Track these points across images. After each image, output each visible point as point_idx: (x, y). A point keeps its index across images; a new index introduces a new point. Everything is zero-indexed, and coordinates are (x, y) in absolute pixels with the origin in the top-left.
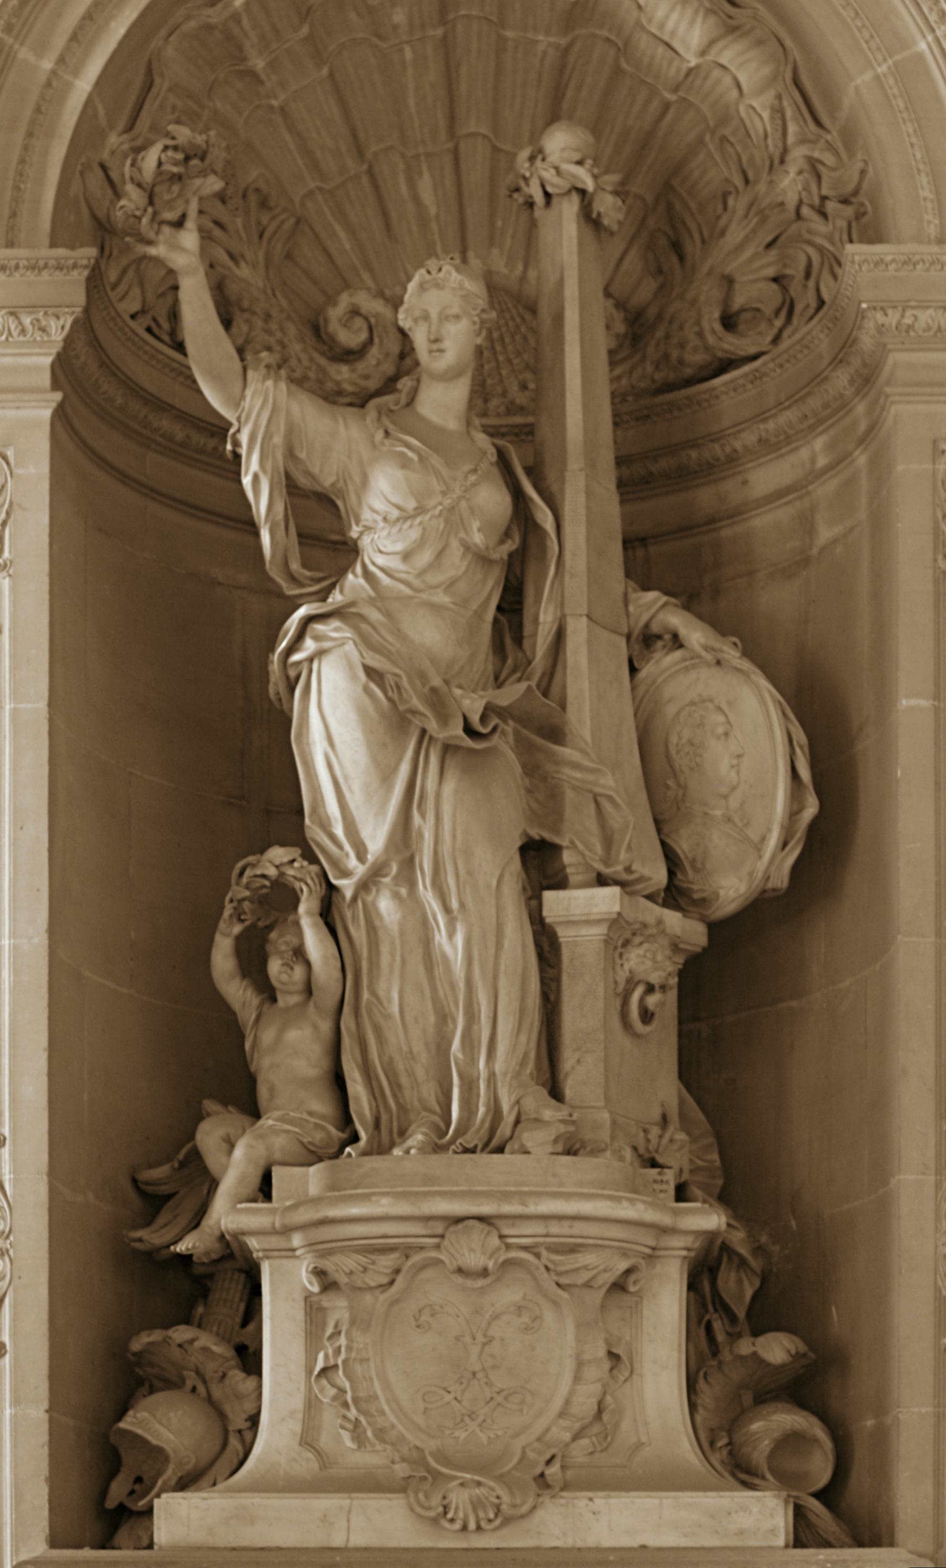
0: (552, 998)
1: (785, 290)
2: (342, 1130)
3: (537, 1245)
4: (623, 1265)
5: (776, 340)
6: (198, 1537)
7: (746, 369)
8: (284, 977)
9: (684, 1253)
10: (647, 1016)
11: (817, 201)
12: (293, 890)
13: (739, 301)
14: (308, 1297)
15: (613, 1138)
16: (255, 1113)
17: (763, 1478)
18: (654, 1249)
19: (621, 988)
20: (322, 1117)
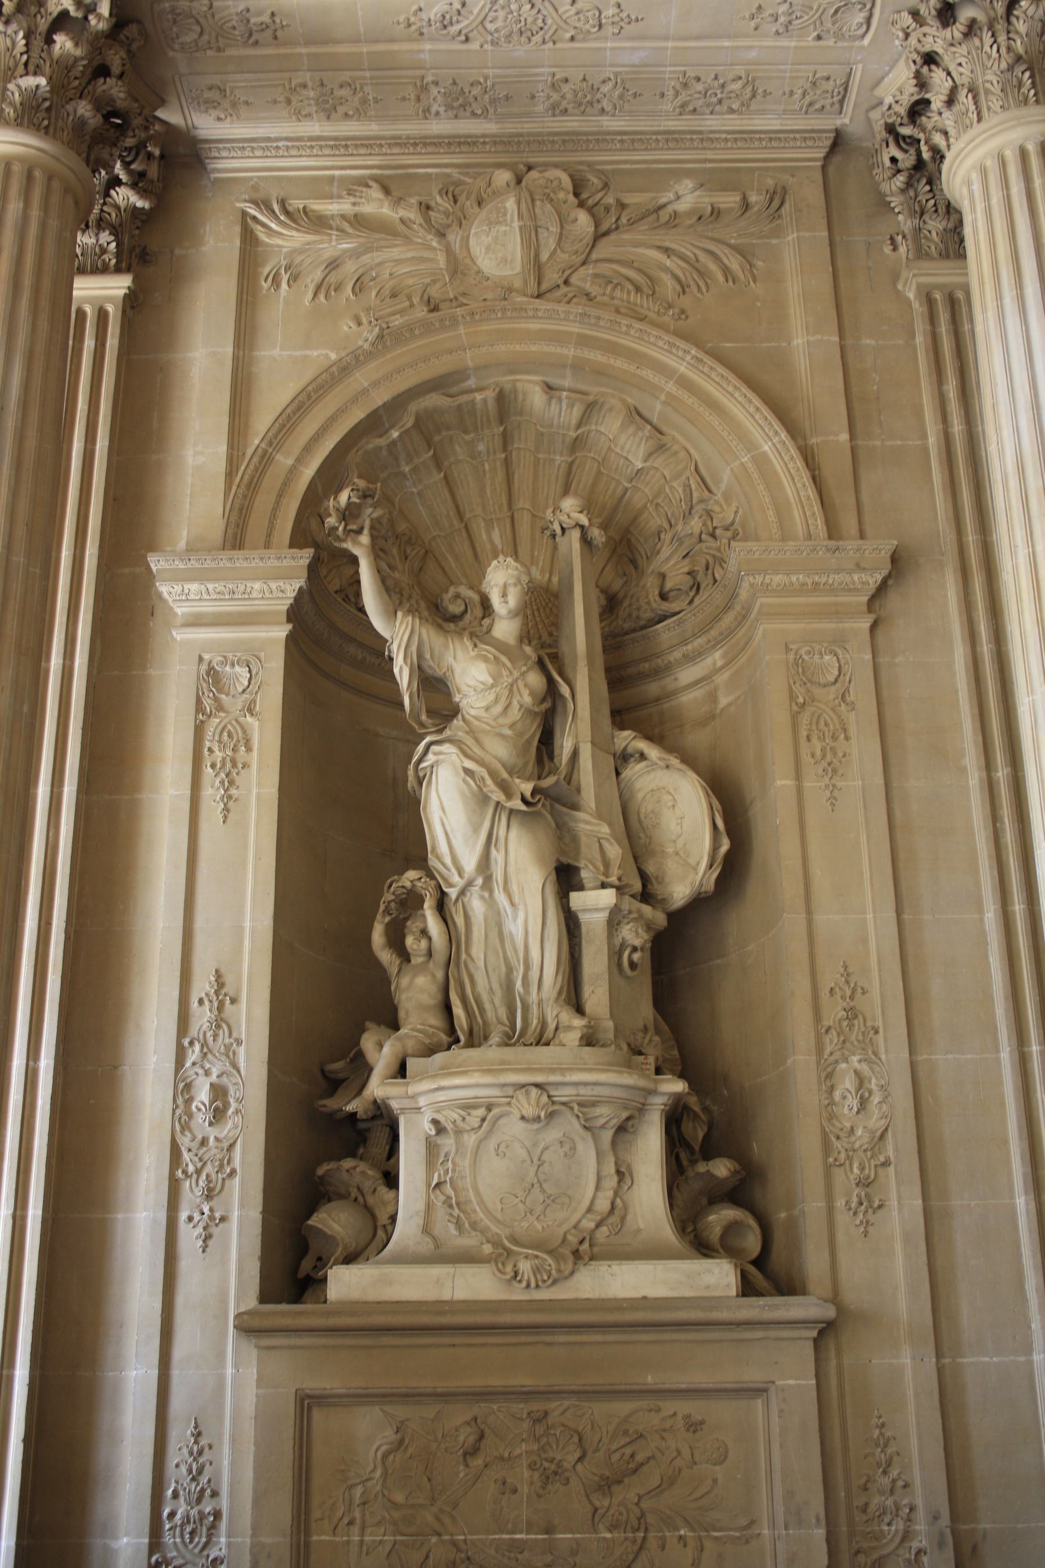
0: (576, 955)
1: (694, 578)
2: (450, 1036)
3: (571, 1102)
4: (625, 1115)
5: (691, 602)
6: (355, 1295)
7: (675, 618)
8: (415, 947)
9: (663, 1107)
10: (633, 965)
11: (711, 529)
12: (421, 895)
13: (668, 585)
14: (428, 1139)
15: (615, 1037)
16: (395, 1026)
17: (717, 1251)
18: (643, 1105)
19: (617, 948)
20: (437, 1028)
